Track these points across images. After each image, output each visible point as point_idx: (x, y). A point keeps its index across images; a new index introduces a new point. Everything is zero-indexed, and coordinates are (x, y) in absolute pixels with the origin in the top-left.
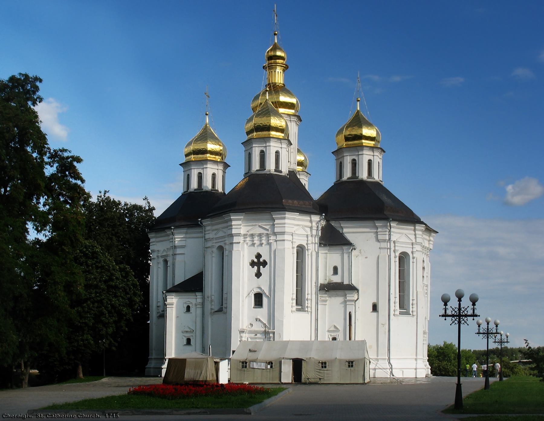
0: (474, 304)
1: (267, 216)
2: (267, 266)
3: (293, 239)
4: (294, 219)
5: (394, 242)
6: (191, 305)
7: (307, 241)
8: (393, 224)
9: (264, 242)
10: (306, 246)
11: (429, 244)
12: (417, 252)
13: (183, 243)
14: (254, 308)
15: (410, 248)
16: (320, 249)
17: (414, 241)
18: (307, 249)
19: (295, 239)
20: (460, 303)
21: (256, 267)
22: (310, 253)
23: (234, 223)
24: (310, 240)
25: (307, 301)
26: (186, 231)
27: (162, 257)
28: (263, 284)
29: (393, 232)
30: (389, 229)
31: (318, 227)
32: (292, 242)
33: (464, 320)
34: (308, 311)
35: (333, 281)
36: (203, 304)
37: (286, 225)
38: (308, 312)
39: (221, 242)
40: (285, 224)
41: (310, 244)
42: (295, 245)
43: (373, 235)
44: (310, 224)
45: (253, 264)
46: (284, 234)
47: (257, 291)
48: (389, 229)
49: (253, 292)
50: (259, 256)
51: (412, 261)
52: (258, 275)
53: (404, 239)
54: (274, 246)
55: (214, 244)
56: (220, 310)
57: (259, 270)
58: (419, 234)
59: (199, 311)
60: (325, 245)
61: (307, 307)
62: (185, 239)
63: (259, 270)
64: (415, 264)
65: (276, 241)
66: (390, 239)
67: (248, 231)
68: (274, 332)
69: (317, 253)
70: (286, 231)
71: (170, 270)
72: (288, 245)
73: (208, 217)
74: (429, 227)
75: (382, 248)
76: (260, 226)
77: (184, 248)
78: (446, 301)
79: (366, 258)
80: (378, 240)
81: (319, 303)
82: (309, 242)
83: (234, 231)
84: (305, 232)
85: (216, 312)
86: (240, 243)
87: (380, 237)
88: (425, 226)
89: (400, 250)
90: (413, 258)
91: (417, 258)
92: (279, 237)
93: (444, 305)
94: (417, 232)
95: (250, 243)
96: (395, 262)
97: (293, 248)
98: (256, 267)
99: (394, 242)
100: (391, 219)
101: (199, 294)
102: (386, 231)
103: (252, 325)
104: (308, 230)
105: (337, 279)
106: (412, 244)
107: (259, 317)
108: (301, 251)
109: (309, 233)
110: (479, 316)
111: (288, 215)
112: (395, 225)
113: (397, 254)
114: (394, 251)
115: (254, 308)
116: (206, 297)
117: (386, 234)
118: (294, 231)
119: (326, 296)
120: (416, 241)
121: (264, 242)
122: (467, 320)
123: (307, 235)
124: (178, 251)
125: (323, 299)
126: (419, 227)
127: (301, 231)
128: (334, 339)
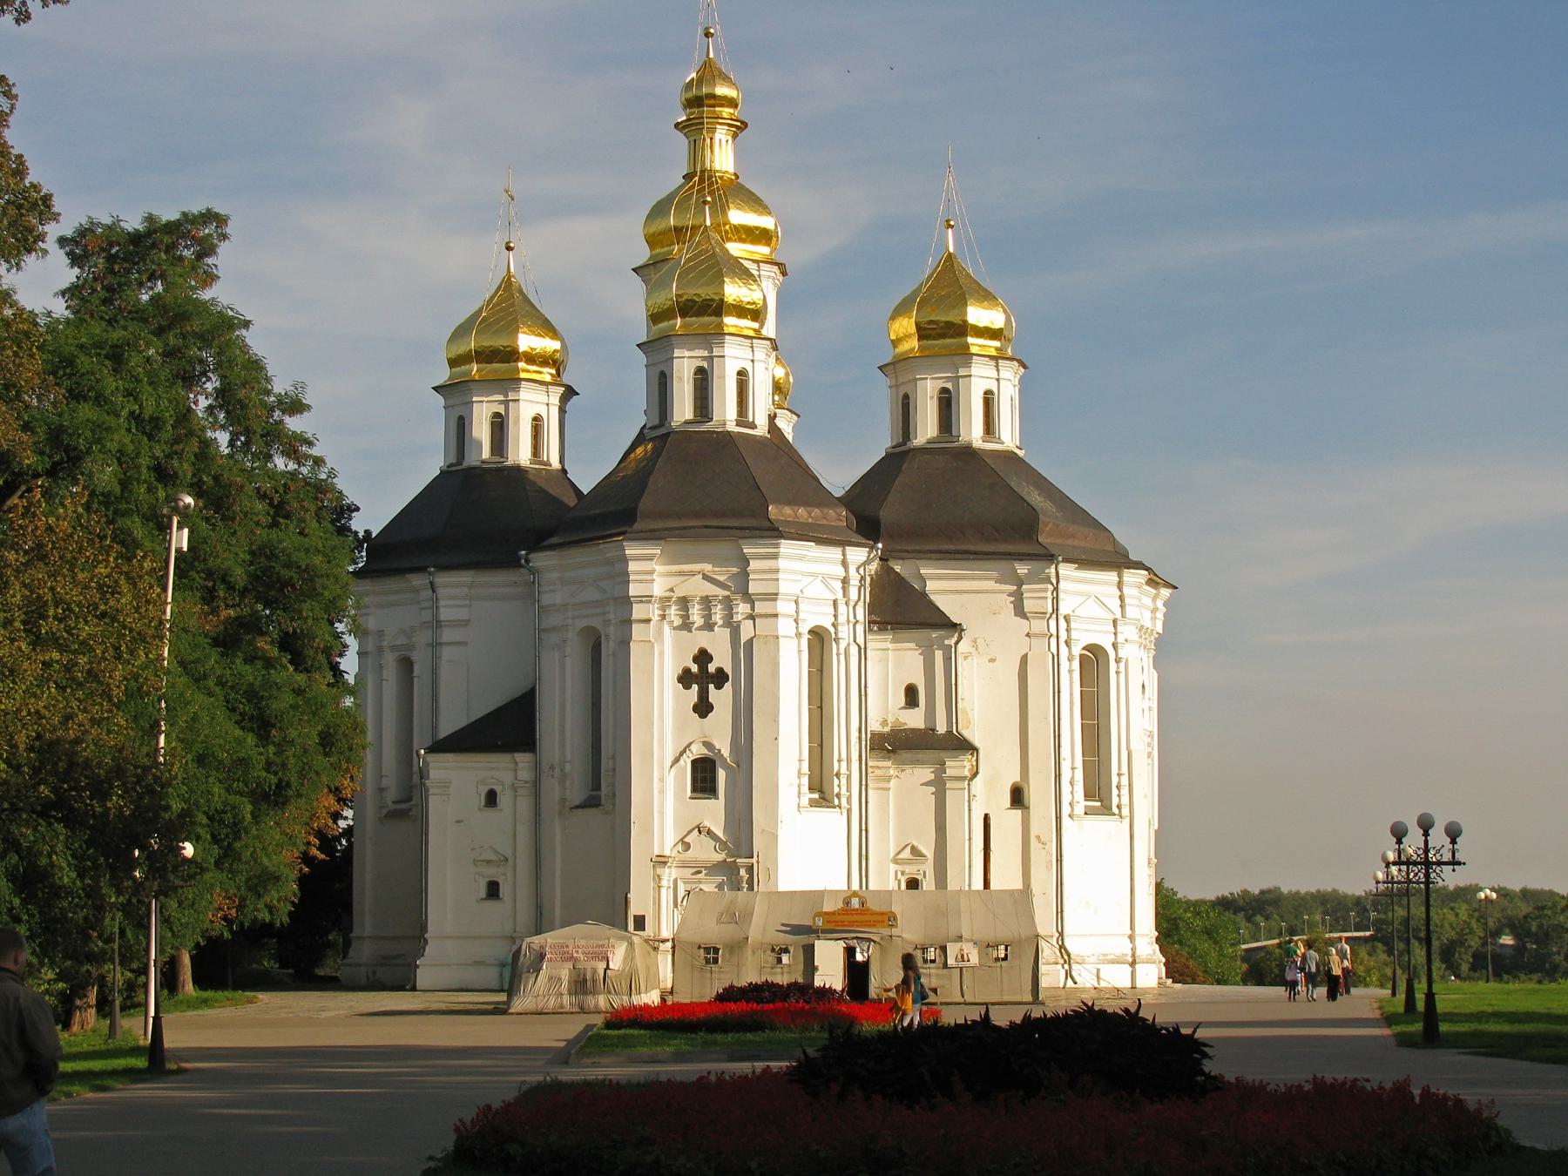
0: (1453, 842)
1: (723, 548)
2: (728, 686)
3: (797, 612)
4: (801, 558)
6: (498, 789)
7: (836, 616)
8: (1066, 570)
9: (718, 616)
11: (1154, 619)
12: (1127, 645)
13: (462, 614)
14: (691, 798)
16: (869, 637)
17: (1119, 616)
18: (837, 640)
20: (1426, 838)
21: (695, 687)
22: (842, 651)
23: (633, 566)
25: (838, 778)
26: (470, 579)
27: (393, 648)
29: (1065, 592)
30: (1055, 582)
31: (863, 578)
33: (1435, 871)
34: (842, 805)
35: (905, 724)
36: (536, 786)
38: (840, 808)
39: (592, 616)
42: (805, 629)
43: (1007, 603)
47: (698, 751)
48: (1052, 584)
49: (691, 755)
50: (703, 657)
51: (1115, 669)
52: (703, 708)
53: (1091, 609)
54: (747, 631)
55: (570, 622)
56: (592, 802)
58: (1132, 597)
59: (524, 806)
60: (882, 630)
61: (838, 795)
62: (467, 602)
64: (1122, 676)
65: (752, 617)
66: (1056, 610)
67: (672, 590)
68: (753, 864)
69: (863, 652)
72: (785, 627)
73: (551, 547)
74: (1156, 575)
75: (1036, 635)
76: (706, 577)
77: (466, 625)
78: (1399, 833)
79: (992, 660)
80: (1020, 612)
81: (870, 785)
82: (842, 619)
83: (633, 590)
84: (829, 593)
85: (577, 807)
86: (652, 622)
87: (1029, 605)
88: (1146, 573)
89: (1082, 639)
90: (1118, 661)
91: (1127, 660)
92: (761, 608)
93: (1396, 843)
94: (1125, 590)
95: (677, 622)
96: (1070, 671)
97: (799, 635)
98: (695, 687)
99: (1067, 618)
100: (1060, 558)
101: (523, 759)
102: (1046, 590)
103: (687, 847)
105: (915, 719)
106: (1115, 622)
107: (707, 823)
110: (1464, 864)
111: (787, 547)
113: (1077, 650)
114: (1067, 643)
115: (691, 798)
116: (545, 767)
118: (801, 591)
119: (889, 763)
120: (1123, 616)
121: (718, 616)
122: (1441, 871)
123: (835, 602)
124: (447, 635)
125: (878, 772)
126: (1134, 578)
128: (913, 884)
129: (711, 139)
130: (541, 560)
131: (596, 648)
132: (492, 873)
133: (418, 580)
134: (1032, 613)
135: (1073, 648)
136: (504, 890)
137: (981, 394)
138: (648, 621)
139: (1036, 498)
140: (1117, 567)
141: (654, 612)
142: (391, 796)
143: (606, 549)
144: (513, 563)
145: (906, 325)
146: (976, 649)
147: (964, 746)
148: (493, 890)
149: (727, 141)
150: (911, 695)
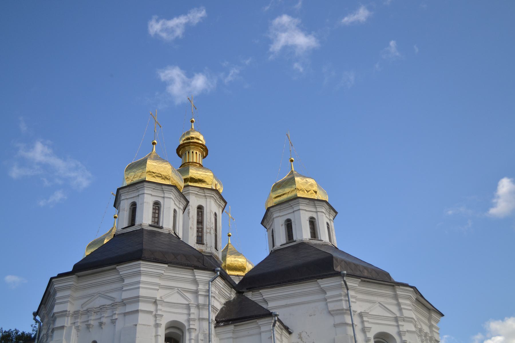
3: (157, 310)
4: (160, 276)
5: (361, 315)
10: (186, 324)
15: (393, 325)
19: (161, 310)
23: (59, 295)
24: (194, 313)
32: (155, 316)
37: (141, 285)
40: (139, 282)
41: (194, 320)
42: (164, 322)
44: (193, 287)
46: (138, 301)
58: (405, 304)
66: (350, 307)
70: (140, 295)
82: (192, 316)
84: (185, 301)
88: (412, 289)
95: (83, 326)
97: (157, 325)
102: (340, 295)
104: (189, 296)
106: (396, 319)
109: (192, 301)
112: (357, 285)
114: (364, 330)
117: (341, 300)
127: (176, 298)
129: (189, 152)
134: (333, 311)
135: (368, 334)
137: (307, 218)
138: (62, 327)
146: (302, 340)
149: (196, 153)
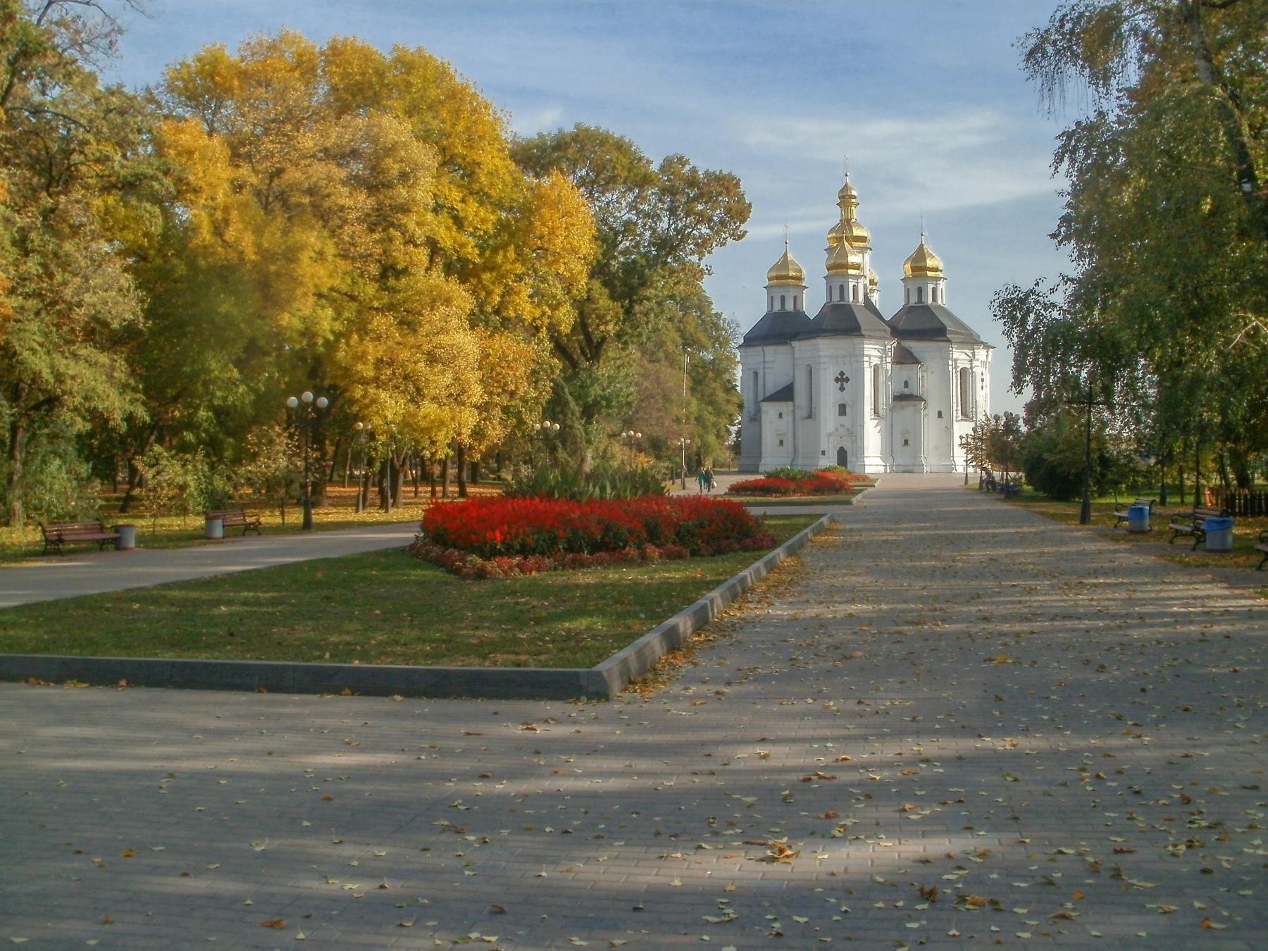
28: (846, 397)
45: (837, 380)
50: (842, 374)
52: (842, 389)
53: (963, 356)
56: (810, 417)
57: (842, 385)
59: (791, 418)
63: (842, 385)
71: (760, 381)
72: (866, 365)
89: (961, 365)
101: (790, 403)
105: (907, 391)
106: (971, 361)
108: (876, 369)
124: (767, 365)
130: (795, 344)
131: (811, 370)
132: (781, 438)
133: (759, 349)
136: (785, 443)
139: (946, 322)
140: (968, 343)
141: (826, 360)
142: (752, 414)
143: (814, 341)
144: (786, 343)
145: (908, 266)
147: (920, 399)
148: (781, 443)
150: (906, 384)
